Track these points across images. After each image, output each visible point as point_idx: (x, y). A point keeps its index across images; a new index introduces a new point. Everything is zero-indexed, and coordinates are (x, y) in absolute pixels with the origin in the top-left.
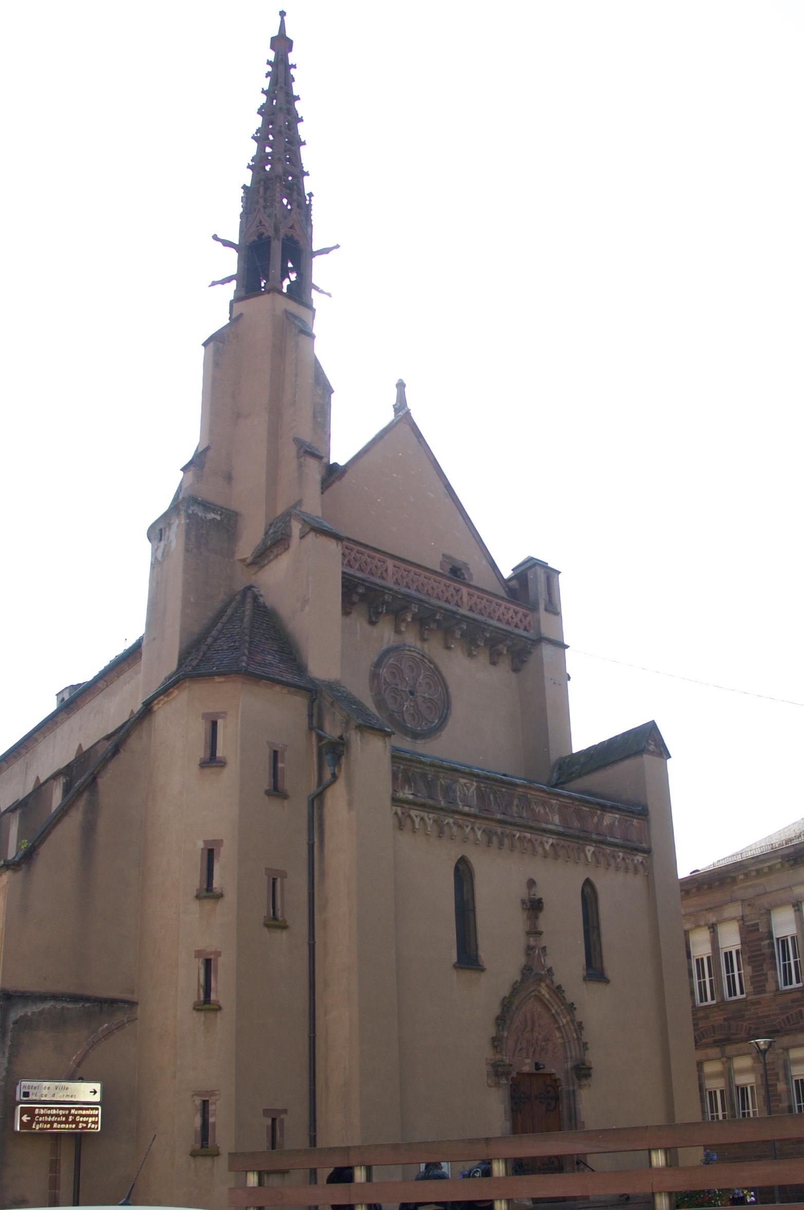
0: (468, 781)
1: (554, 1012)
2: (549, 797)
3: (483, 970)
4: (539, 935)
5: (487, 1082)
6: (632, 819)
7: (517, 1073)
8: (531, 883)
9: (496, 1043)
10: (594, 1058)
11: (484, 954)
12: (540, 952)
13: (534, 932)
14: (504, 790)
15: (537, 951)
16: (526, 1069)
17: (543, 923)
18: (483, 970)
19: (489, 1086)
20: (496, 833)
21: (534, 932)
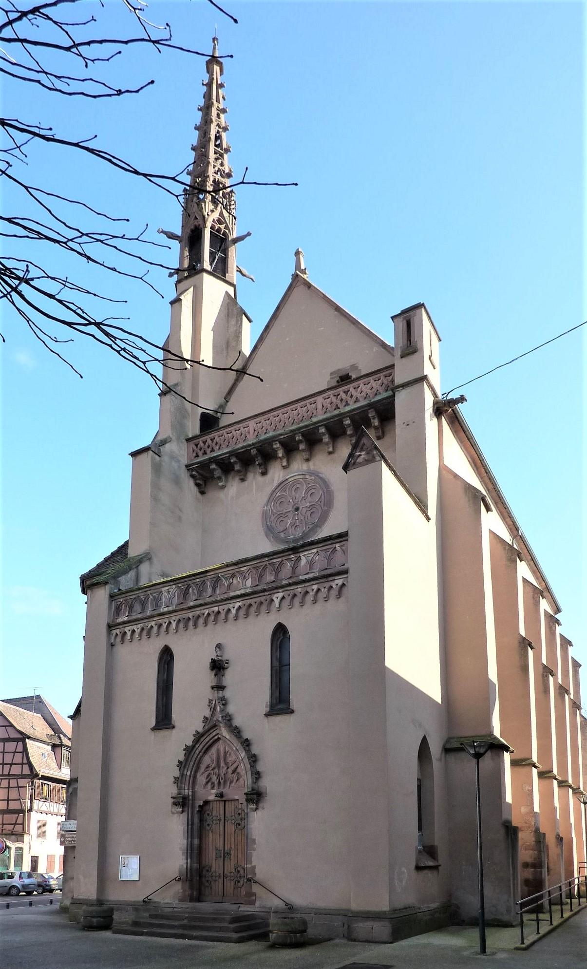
0: (169, 587)
1: (234, 748)
2: (236, 567)
3: (174, 727)
4: (222, 689)
5: (172, 811)
6: (333, 546)
7: (204, 802)
8: (219, 646)
9: (177, 781)
10: (267, 783)
11: (175, 716)
12: (217, 703)
13: (219, 687)
14: (198, 580)
15: (214, 702)
16: (212, 798)
17: (229, 678)
18: (174, 727)
19: (173, 813)
20: (189, 619)
21: (219, 687)
